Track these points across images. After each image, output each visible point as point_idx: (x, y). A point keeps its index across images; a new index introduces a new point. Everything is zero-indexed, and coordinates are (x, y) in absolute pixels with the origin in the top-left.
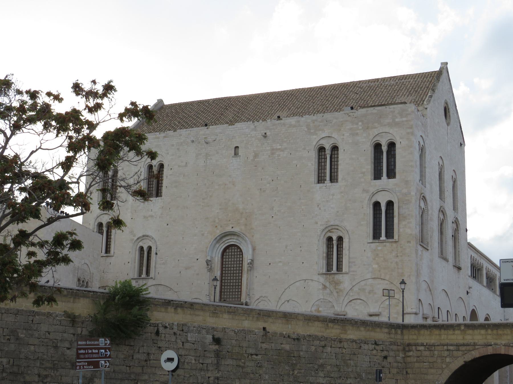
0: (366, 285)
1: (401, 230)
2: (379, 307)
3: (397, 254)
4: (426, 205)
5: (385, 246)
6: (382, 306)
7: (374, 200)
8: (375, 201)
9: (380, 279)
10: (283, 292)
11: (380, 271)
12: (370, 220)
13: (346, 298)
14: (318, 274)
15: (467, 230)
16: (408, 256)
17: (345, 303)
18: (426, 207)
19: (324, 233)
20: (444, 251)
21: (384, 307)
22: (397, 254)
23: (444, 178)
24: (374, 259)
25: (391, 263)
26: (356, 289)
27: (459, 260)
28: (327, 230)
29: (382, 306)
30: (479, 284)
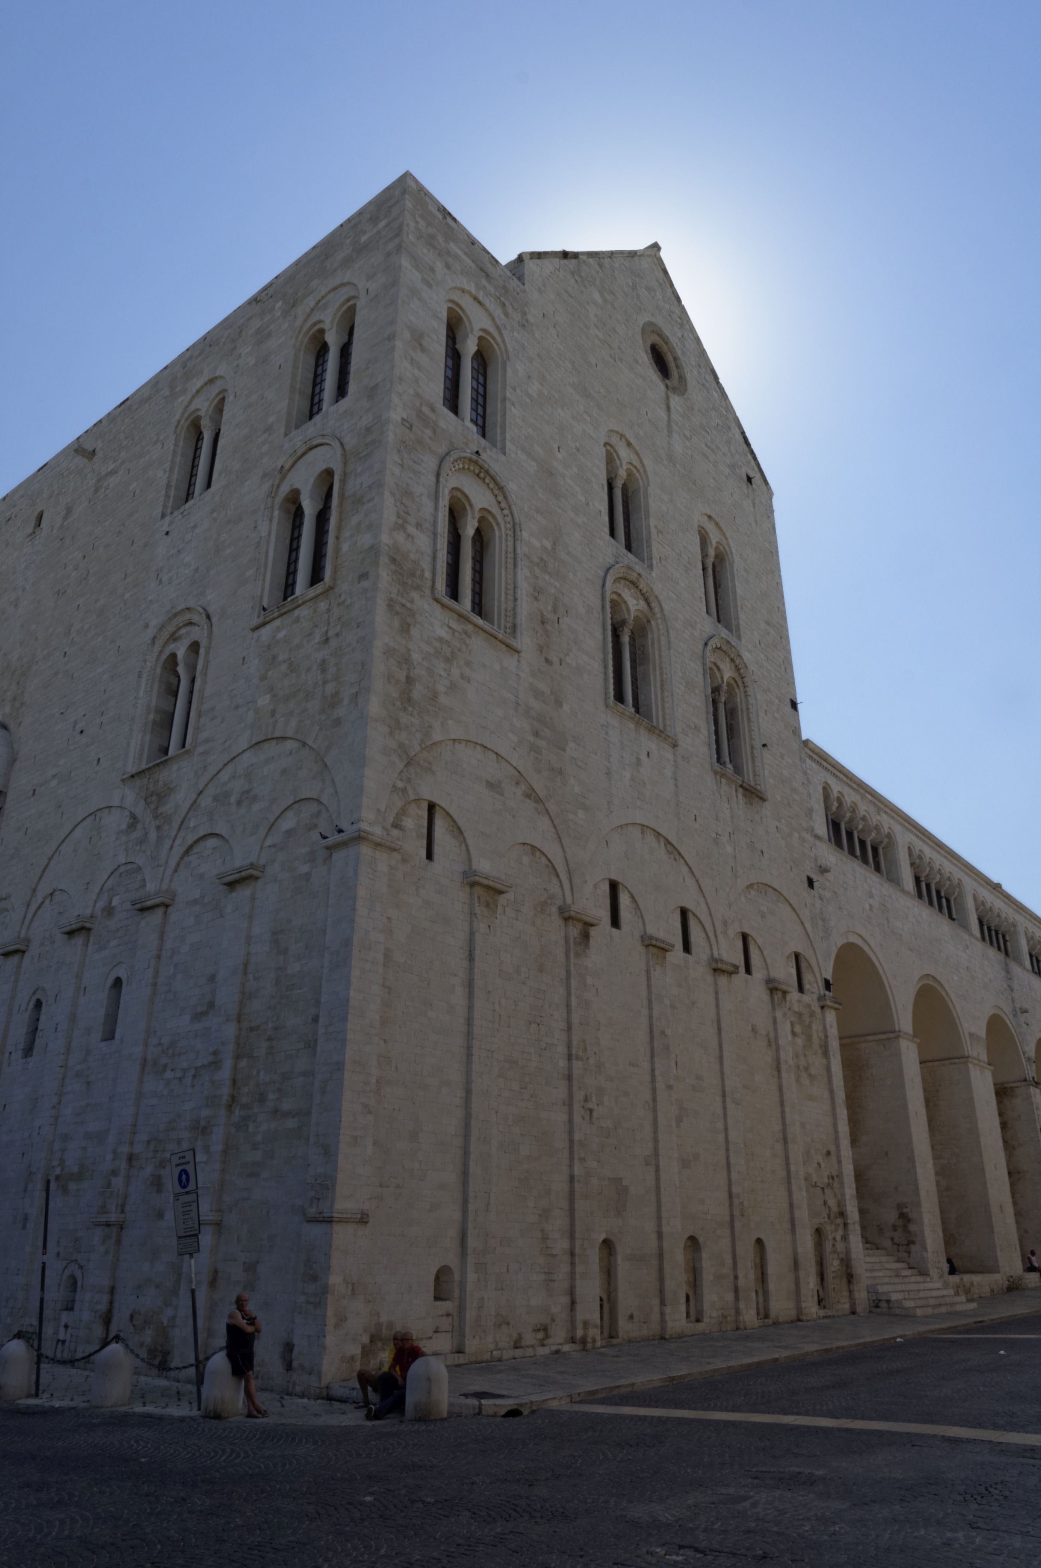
0: (233, 777)
1: (345, 547)
2: (262, 848)
3: (327, 632)
4: (503, 505)
5: (297, 620)
6: (269, 842)
7: (285, 489)
8: (316, 513)
9: (275, 741)
10: (44, 871)
11: (273, 713)
12: (267, 557)
13: (178, 842)
14: (123, 781)
15: (794, 705)
16: (358, 627)
17: (173, 863)
18: (506, 512)
19: (157, 649)
20: (642, 697)
21: (274, 846)
22: (327, 632)
23: (647, 505)
24: (263, 678)
25: (308, 670)
26: (206, 801)
27: (754, 772)
28: (166, 635)
29: (269, 842)
30: (874, 878)
